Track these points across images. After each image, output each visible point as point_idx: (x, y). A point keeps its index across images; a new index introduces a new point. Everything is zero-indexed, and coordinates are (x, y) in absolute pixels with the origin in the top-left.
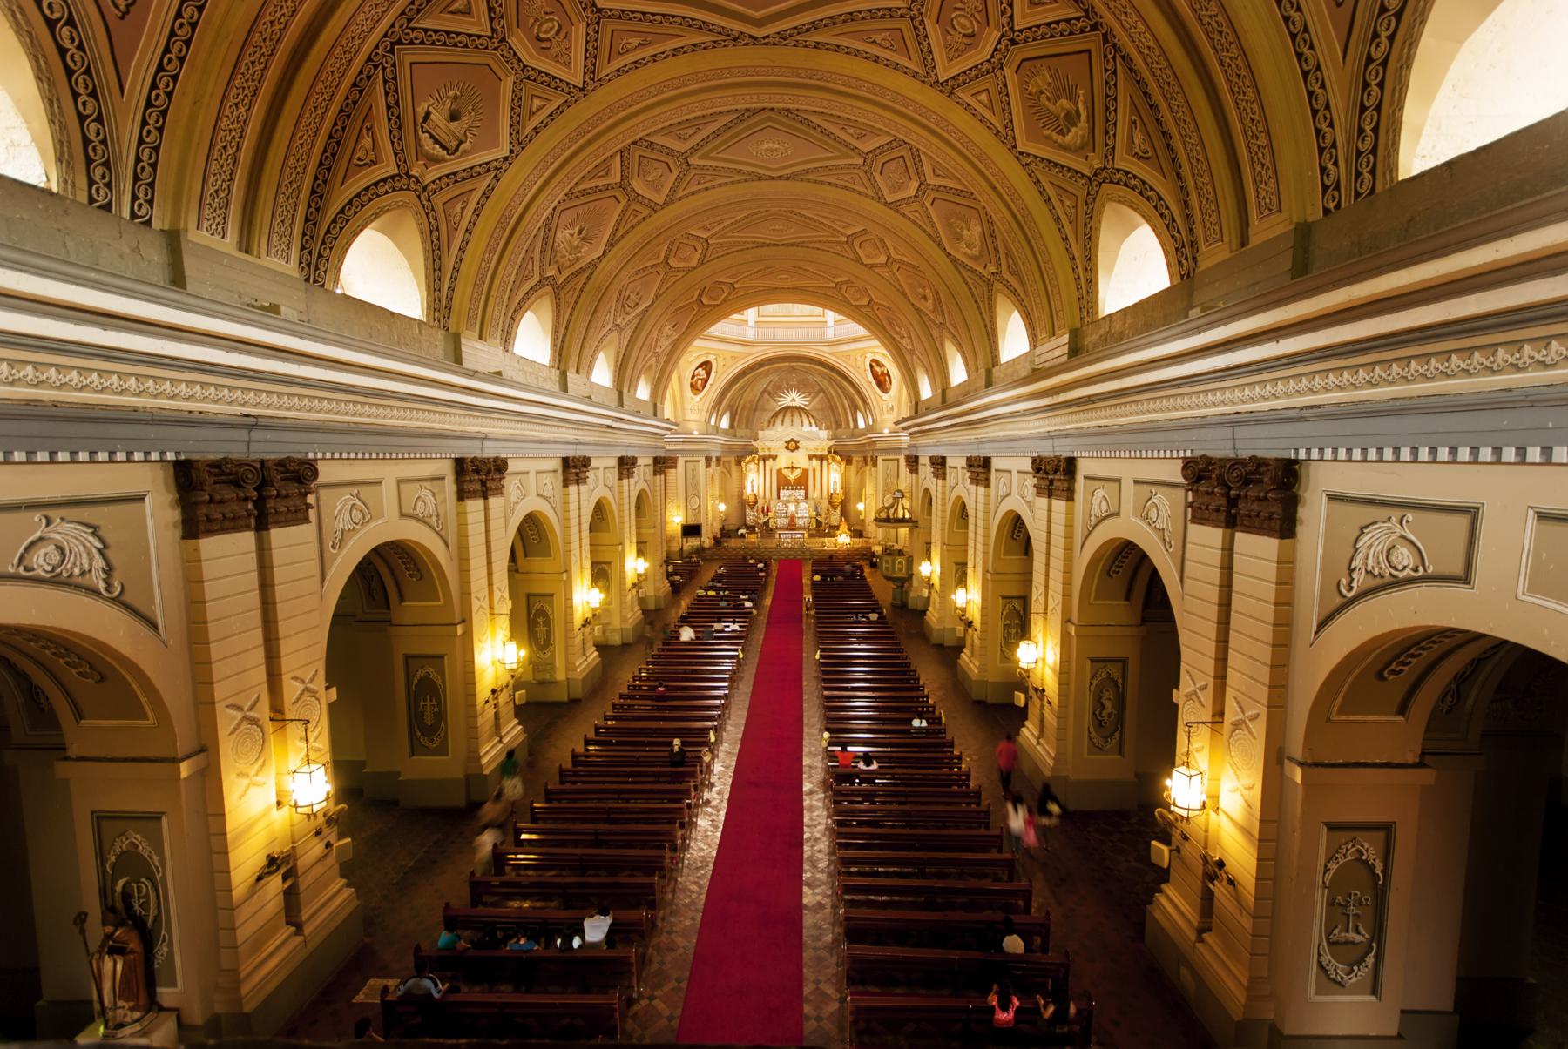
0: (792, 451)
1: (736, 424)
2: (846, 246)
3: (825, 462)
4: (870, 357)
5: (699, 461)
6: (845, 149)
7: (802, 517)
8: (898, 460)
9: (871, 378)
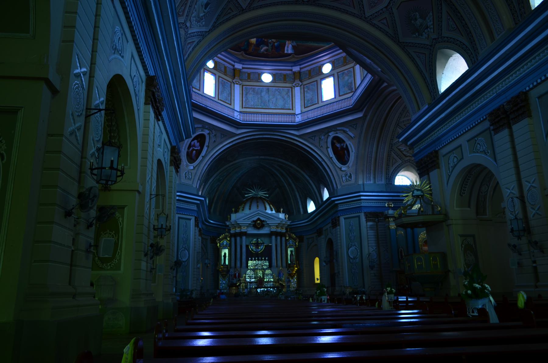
0: (259, 229)
1: (212, 210)
3: (283, 239)
4: (332, 134)
5: (190, 219)
7: (268, 282)
8: (359, 217)
9: (332, 155)
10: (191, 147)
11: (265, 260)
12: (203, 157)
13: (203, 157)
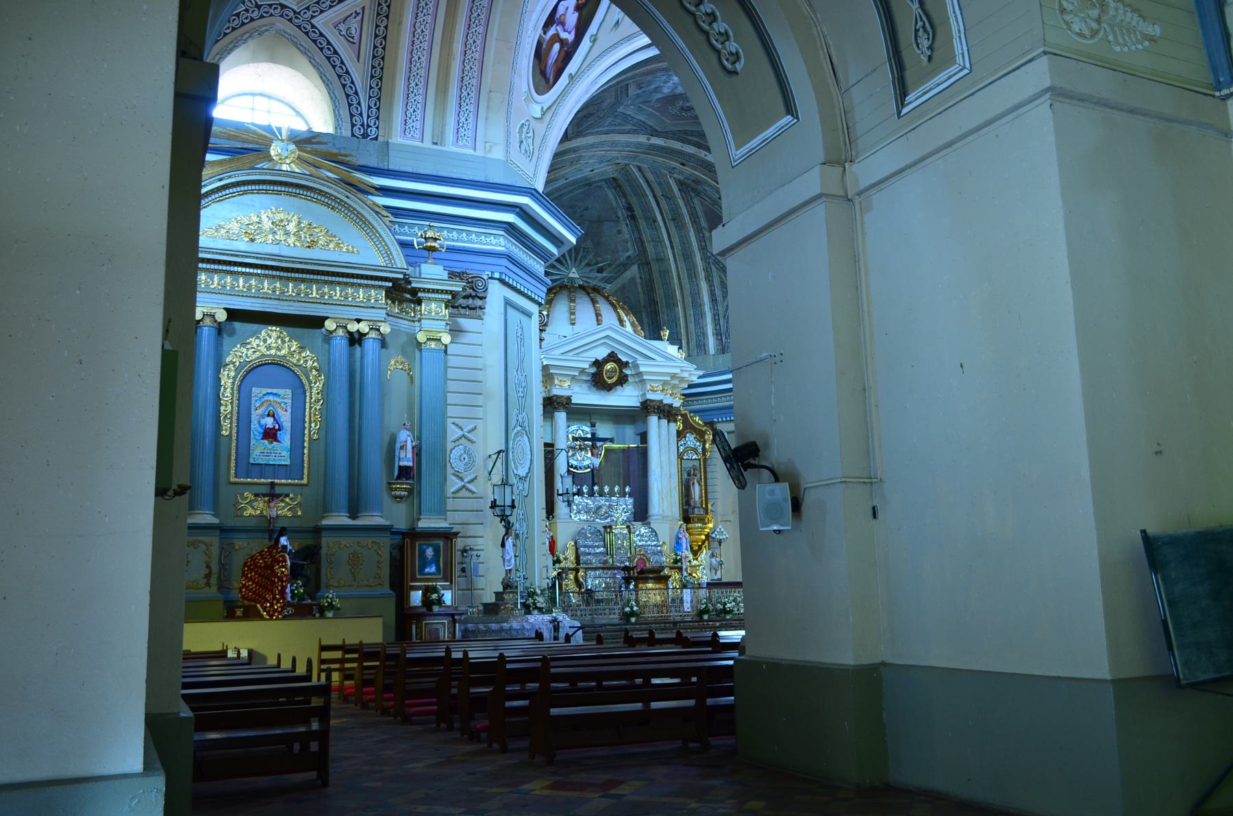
0: (608, 388)
10: (555, 22)
11: (623, 494)
12: (571, 77)
13: (571, 77)
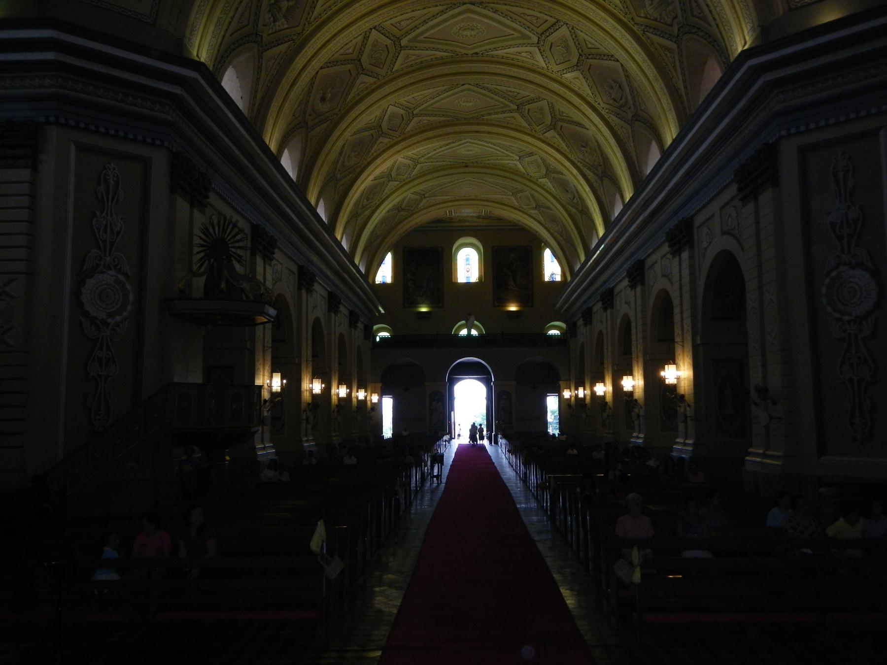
2: (398, 33)
6: (425, 112)
